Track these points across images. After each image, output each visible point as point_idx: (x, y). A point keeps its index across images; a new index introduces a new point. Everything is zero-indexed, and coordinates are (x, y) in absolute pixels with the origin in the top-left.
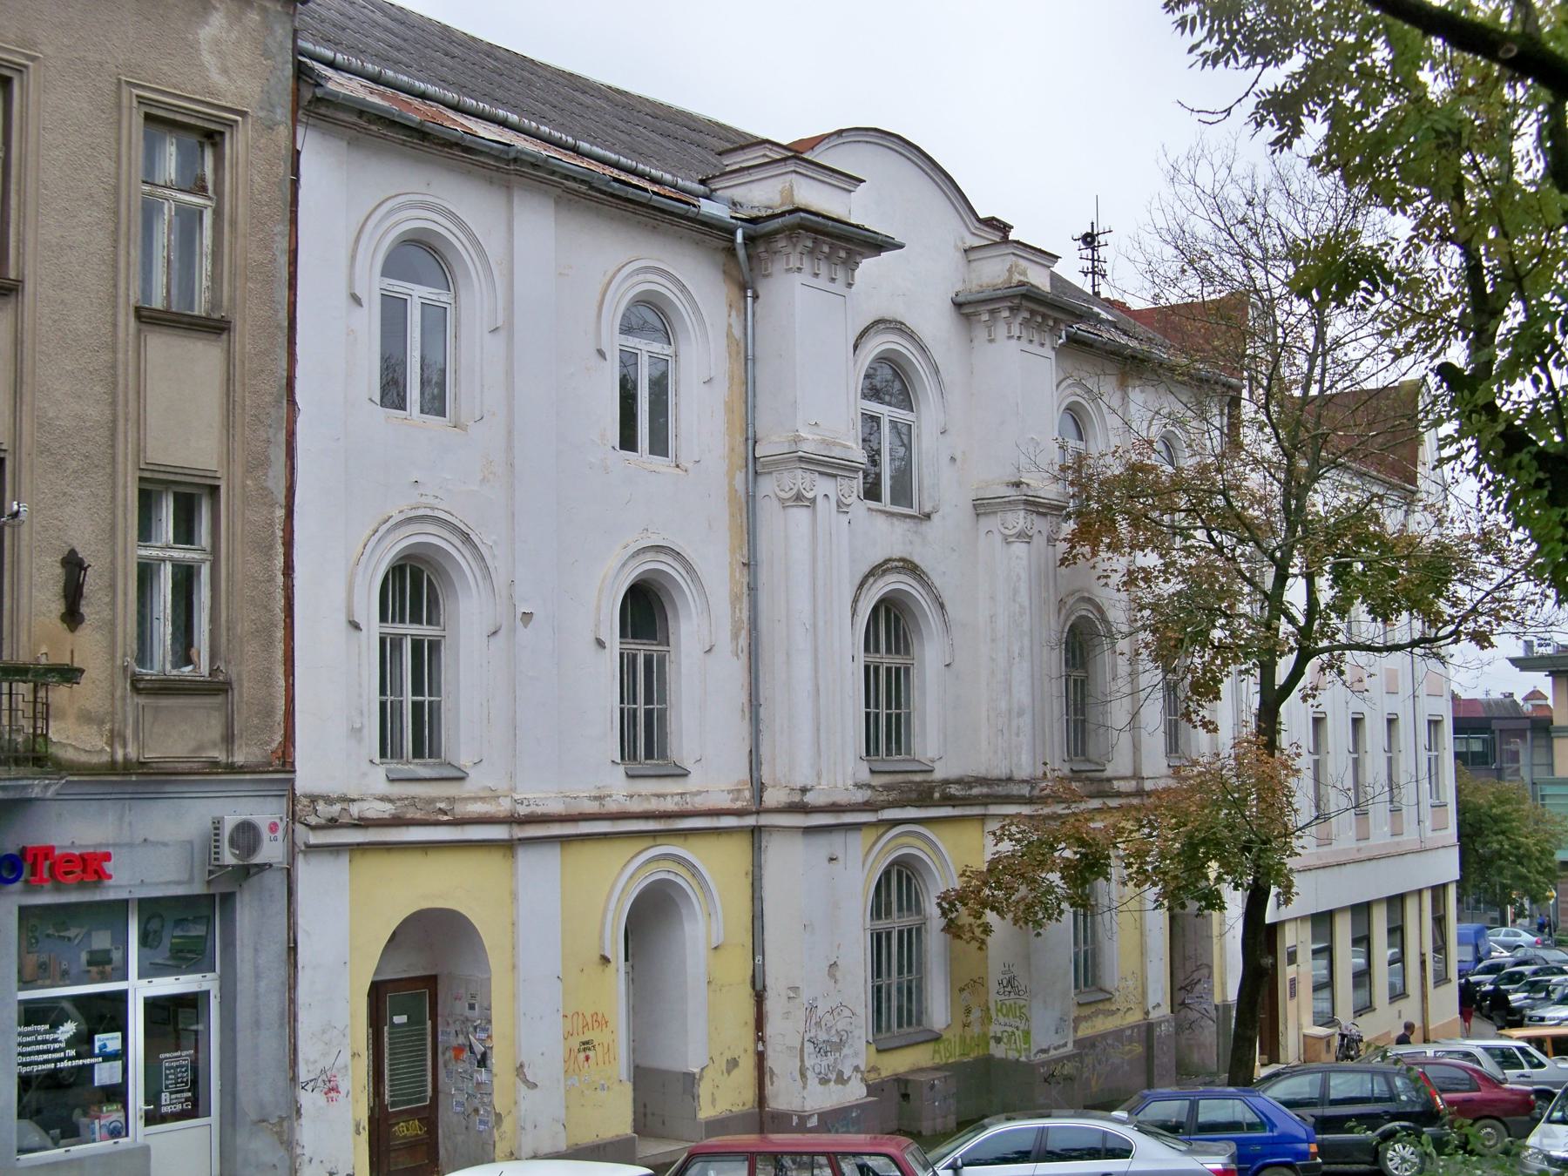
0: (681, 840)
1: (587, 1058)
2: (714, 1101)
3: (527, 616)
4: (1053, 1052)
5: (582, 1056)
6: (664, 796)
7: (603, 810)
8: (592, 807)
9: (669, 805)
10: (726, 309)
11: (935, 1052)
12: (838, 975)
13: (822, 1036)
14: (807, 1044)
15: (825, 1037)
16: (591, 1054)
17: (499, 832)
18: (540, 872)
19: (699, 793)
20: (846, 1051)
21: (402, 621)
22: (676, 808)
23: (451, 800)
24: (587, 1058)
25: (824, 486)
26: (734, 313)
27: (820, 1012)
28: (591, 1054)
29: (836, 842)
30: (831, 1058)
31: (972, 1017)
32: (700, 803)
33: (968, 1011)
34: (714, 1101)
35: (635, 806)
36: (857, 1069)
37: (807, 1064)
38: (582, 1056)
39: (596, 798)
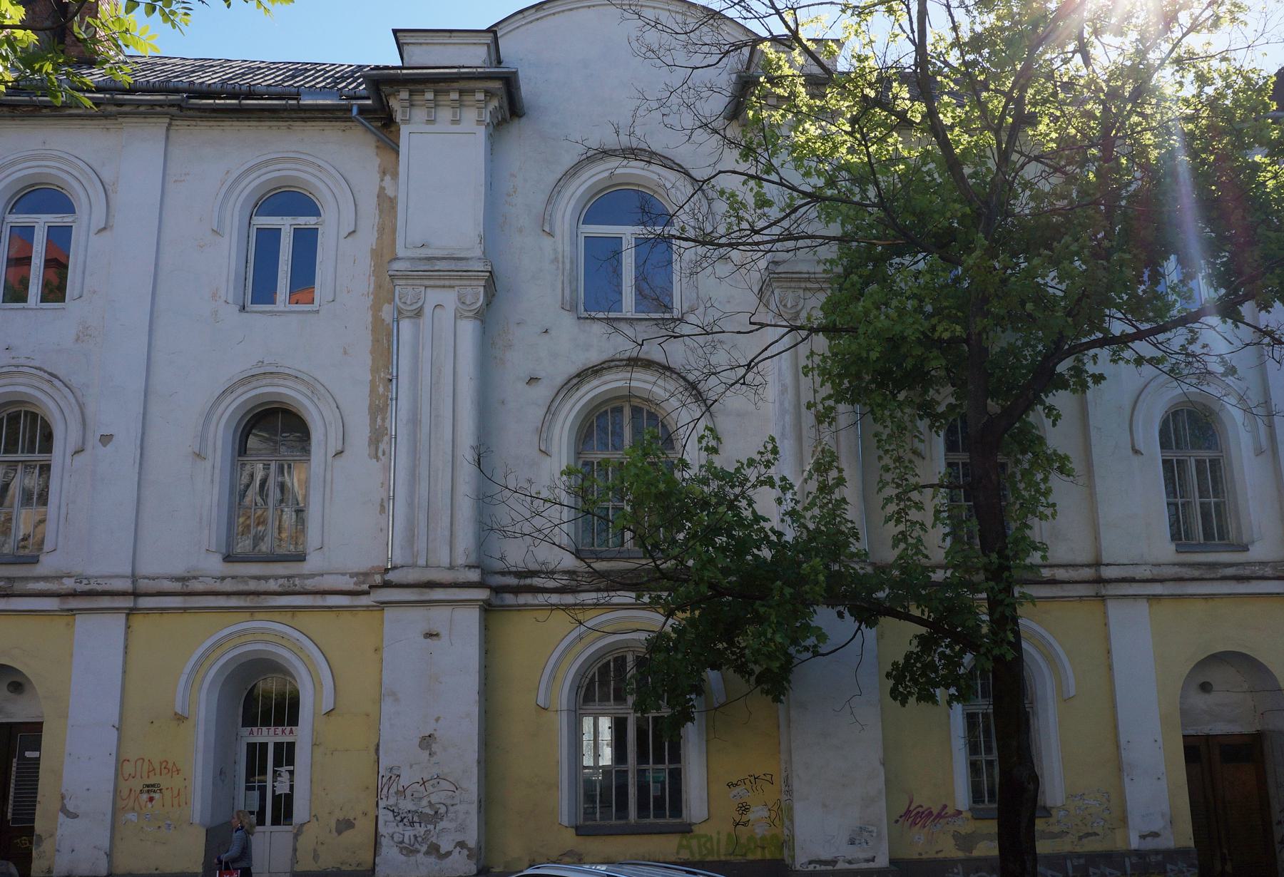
0: (287, 617)
1: (151, 799)
2: (316, 857)
3: (106, 439)
4: (841, 866)
5: (145, 796)
6: (266, 578)
7: (185, 590)
8: (177, 586)
9: (272, 585)
10: (377, 177)
11: (680, 846)
12: (435, 747)
13: (406, 805)
14: (381, 811)
15: (414, 808)
16: (157, 796)
17: (52, 604)
18: (99, 637)
19: (313, 576)
20: (441, 825)
21: (32, 450)
22: (280, 589)
23: (10, 579)
24: (151, 799)
25: (433, 297)
26: (388, 178)
27: (404, 781)
28: (157, 796)
29: (438, 617)
30: (420, 830)
31: (751, 816)
32: (310, 584)
33: (744, 808)
34: (316, 857)
35: (228, 586)
36: (461, 844)
37: (382, 830)
38: (145, 796)
39: (178, 579)
